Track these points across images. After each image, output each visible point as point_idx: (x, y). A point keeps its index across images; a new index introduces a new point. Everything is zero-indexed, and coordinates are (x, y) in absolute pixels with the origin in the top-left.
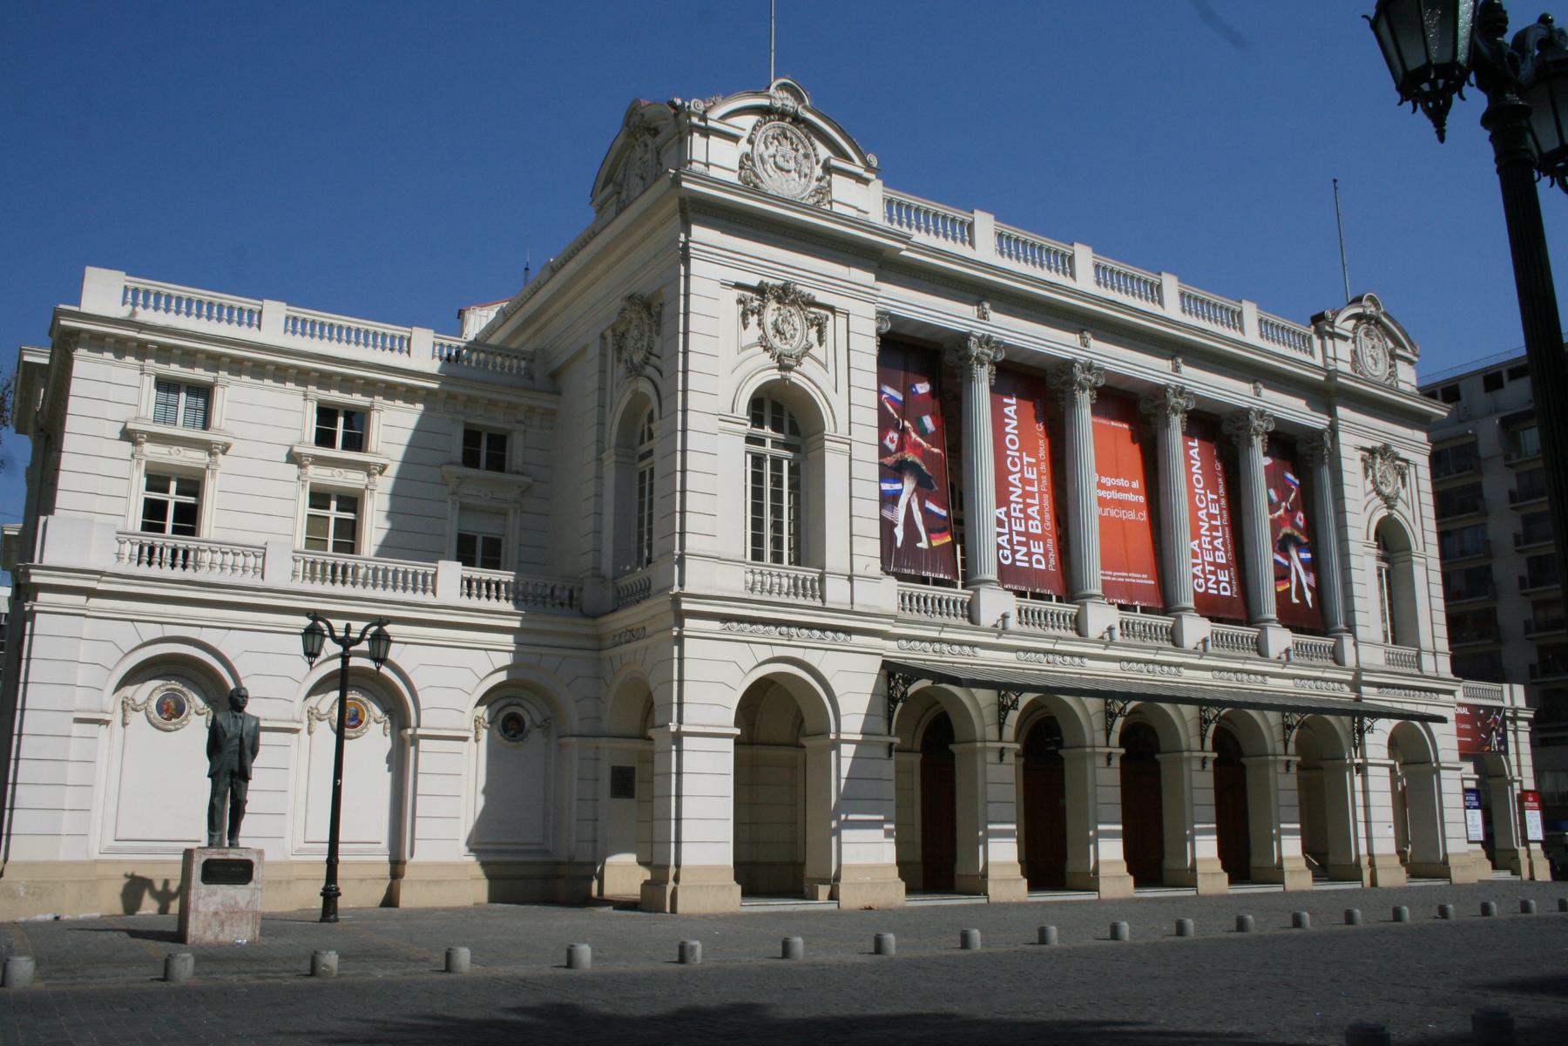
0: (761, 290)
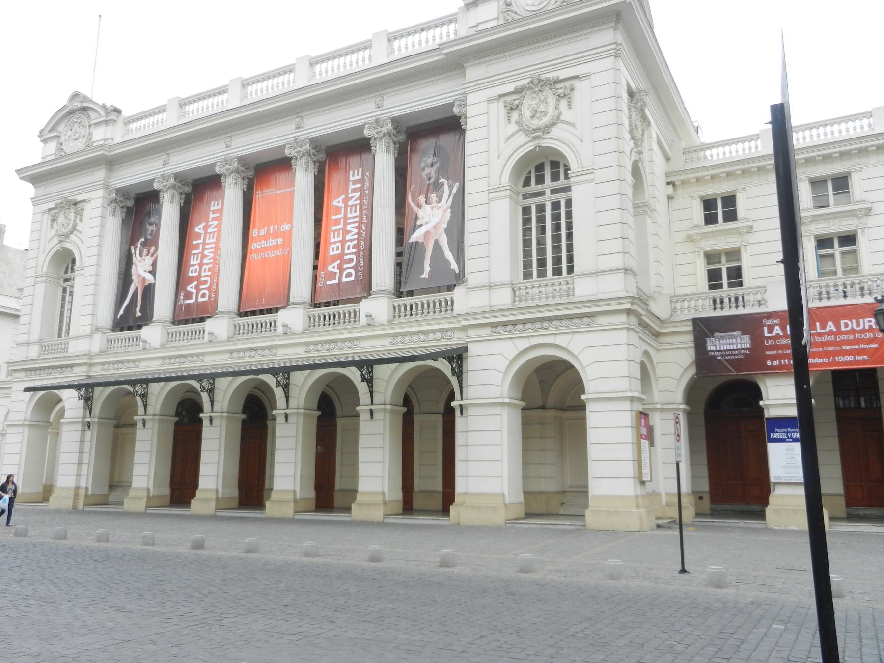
0: (518, 91)
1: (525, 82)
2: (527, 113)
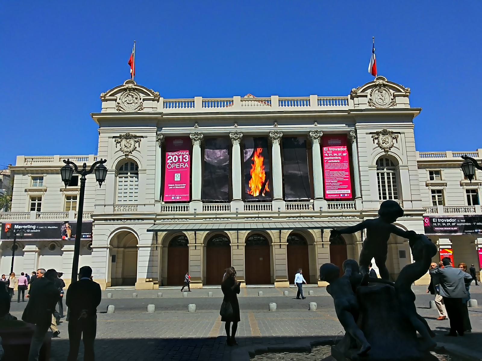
1: (381, 130)
2: (381, 142)
